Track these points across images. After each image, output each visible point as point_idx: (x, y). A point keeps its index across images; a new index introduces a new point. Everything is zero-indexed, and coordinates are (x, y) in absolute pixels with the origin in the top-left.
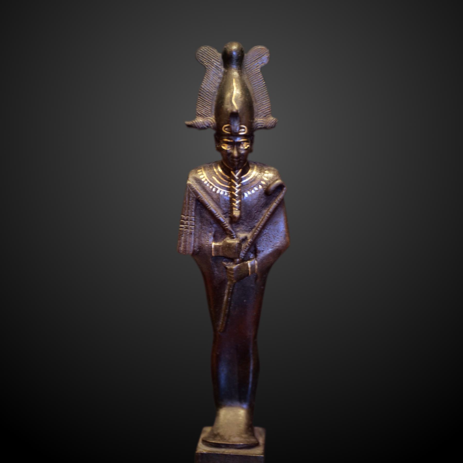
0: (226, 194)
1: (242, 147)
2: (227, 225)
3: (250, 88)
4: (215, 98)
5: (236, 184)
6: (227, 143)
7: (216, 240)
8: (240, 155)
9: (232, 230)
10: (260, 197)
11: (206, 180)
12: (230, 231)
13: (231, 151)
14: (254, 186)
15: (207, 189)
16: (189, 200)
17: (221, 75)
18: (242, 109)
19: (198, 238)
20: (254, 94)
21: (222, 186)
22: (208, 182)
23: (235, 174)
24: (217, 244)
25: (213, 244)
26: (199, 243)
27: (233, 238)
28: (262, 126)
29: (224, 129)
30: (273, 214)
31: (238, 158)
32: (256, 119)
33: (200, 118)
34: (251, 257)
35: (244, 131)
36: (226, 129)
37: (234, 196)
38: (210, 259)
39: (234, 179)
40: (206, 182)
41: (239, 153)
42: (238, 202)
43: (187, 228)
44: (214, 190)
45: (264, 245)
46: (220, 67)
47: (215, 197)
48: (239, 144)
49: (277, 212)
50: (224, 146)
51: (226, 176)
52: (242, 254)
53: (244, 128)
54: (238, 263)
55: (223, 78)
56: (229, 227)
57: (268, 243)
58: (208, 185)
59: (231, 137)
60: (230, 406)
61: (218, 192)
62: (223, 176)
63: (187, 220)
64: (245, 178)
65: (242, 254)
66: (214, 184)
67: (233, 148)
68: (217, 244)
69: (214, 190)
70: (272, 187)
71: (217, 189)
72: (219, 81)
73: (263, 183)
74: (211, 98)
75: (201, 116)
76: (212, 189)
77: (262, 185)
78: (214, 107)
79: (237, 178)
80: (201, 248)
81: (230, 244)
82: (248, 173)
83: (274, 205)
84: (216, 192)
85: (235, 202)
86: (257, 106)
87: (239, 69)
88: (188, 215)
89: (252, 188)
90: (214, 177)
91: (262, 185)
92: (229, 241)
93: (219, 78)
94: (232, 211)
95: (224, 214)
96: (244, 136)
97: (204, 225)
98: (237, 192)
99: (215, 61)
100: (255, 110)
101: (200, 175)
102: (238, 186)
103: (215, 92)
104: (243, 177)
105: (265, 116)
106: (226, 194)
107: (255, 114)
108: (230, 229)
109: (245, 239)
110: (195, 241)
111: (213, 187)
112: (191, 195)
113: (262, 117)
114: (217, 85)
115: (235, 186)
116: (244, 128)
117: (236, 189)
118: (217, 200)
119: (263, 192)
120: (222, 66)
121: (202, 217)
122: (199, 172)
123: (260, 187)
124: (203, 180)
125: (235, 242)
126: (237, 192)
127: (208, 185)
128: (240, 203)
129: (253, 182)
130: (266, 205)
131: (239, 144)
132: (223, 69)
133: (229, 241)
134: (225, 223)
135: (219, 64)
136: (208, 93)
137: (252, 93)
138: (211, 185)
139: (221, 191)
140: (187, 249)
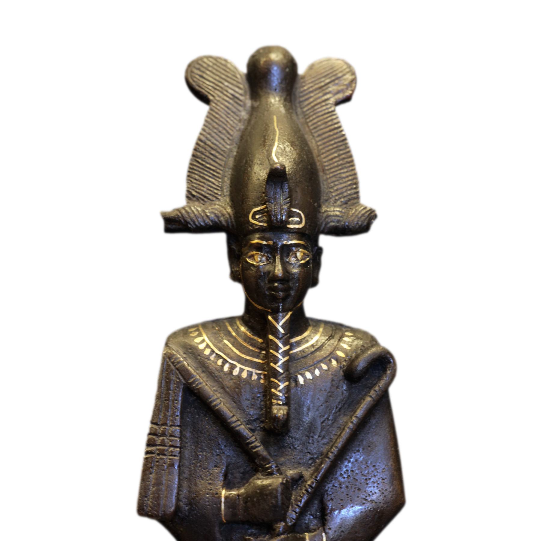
0: (255, 377)
1: (293, 260)
2: (257, 444)
3: (313, 144)
4: (231, 162)
5: (280, 345)
6: (259, 248)
7: (228, 485)
8: (287, 277)
9: (269, 457)
10: (335, 386)
11: (208, 346)
12: (264, 459)
13: (268, 268)
14: (321, 361)
15: (212, 367)
16: (169, 389)
17: (244, 115)
18: (296, 172)
19: (189, 480)
20: (319, 156)
21: (246, 360)
22: (213, 351)
23: (277, 321)
24: (234, 493)
25: (224, 492)
26: (189, 492)
27: (271, 474)
28: (338, 221)
29: (254, 217)
30: (363, 423)
31: (282, 280)
32: (324, 209)
33: (197, 203)
34: (311, 527)
35: (300, 223)
36: (257, 217)
37: (275, 374)
38: (217, 529)
39: (275, 332)
40: (207, 352)
41: (285, 269)
42: (282, 386)
43: (162, 453)
44: (226, 368)
45: (343, 496)
46: (241, 98)
47: (228, 383)
48: (287, 250)
49: (373, 421)
50: (252, 257)
51: (256, 338)
52: (292, 515)
53: (299, 215)
54: (282, 534)
55: (249, 120)
56: (260, 449)
57: (351, 493)
58: (212, 358)
59: (267, 235)
60: (374, 357)
61: (236, 372)
62: (247, 339)
63: (163, 434)
64: (299, 343)
65: (292, 515)
66: (225, 354)
67: (271, 261)
68: (234, 493)
69: (226, 368)
70: (361, 364)
71: (233, 367)
72: (241, 126)
73: (340, 354)
74: (222, 163)
75: (198, 199)
76: (222, 366)
77: (337, 359)
78: (227, 181)
79: (282, 331)
80: (192, 502)
81: (263, 488)
82: (306, 334)
83: (368, 400)
84: (231, 372)
85: (276, 387)
86: (327, 179)
87: (285, 100)
88: (165, 424)
89: (316, 365)
90: (226, 341)
91: (337, 359)
92: (262, 481)
93: (240, 121)
94: (268, 407)
95: (249, 422)
96: (300, 234)
97: (202, 450)
98: (280, 363)
99: (230, 86)
100: (324, 187)
101: (196, 337)
102: (283, 349)
103: (231, 150)
104: (293, 340)
105: (346, 203)
106: (255, 377)
107: (323, 197)
108: (265, 453)
109: (298, 480)
110: (180, 487)
111: (225, 362)
112: (173, 378)
113: (339, 203)
114: (236, 135)
115: (277, 349)
116: (299, 215)
117: (280, 357)
118: (235, 389)
119: (342, 373)
120: (248, 97)
121: (197, 431)
122: (191, 332)
123: (334, 363)
124: (201, 347)
125: (273, 482)
126: (280, 363)
127: (212, 358)
128: (288, 389)
129: (318, 353)
130: (350, 404)
131: (287, 250)
132: (249, 103)
133: (262, 481)
134: (253, 439)
135: (241, 92)
136: (213, 152)
137: (315, 152)
138: (219, 357)
139: (242, 371)
140: (162, 502)
